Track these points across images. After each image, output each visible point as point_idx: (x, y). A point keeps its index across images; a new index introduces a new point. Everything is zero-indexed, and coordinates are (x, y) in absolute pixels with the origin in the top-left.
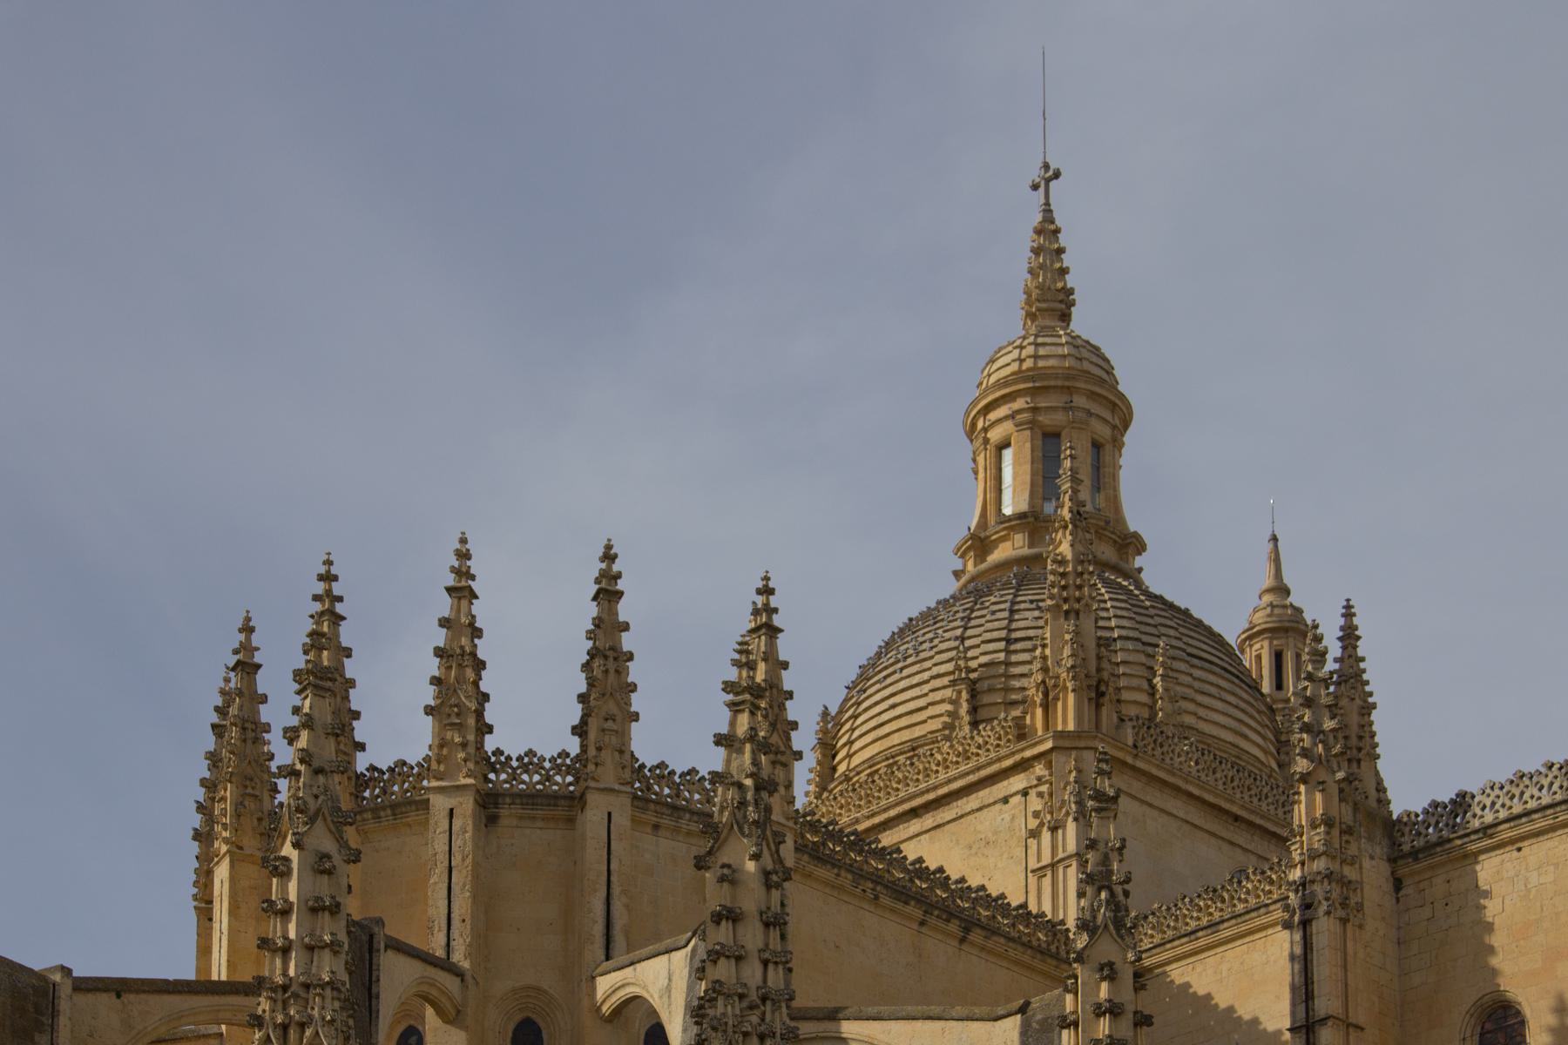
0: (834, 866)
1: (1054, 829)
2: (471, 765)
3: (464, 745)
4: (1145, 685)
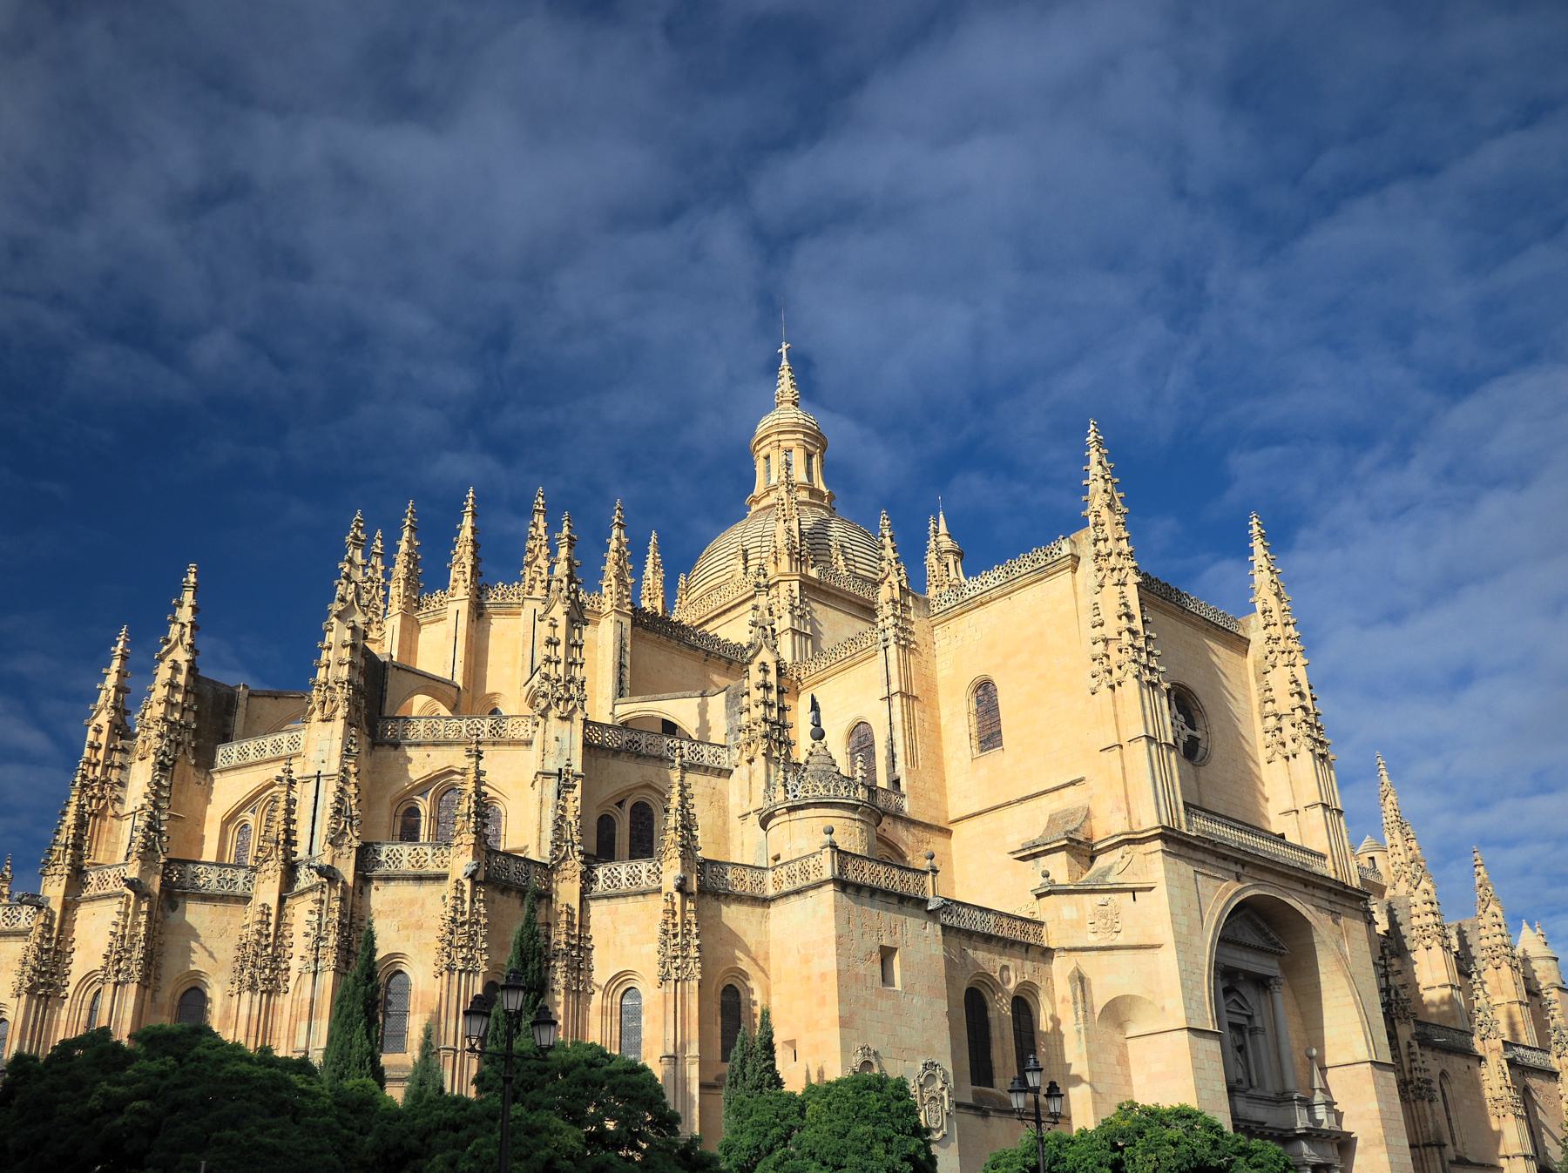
2: (468, 590)
3: (465, 581)
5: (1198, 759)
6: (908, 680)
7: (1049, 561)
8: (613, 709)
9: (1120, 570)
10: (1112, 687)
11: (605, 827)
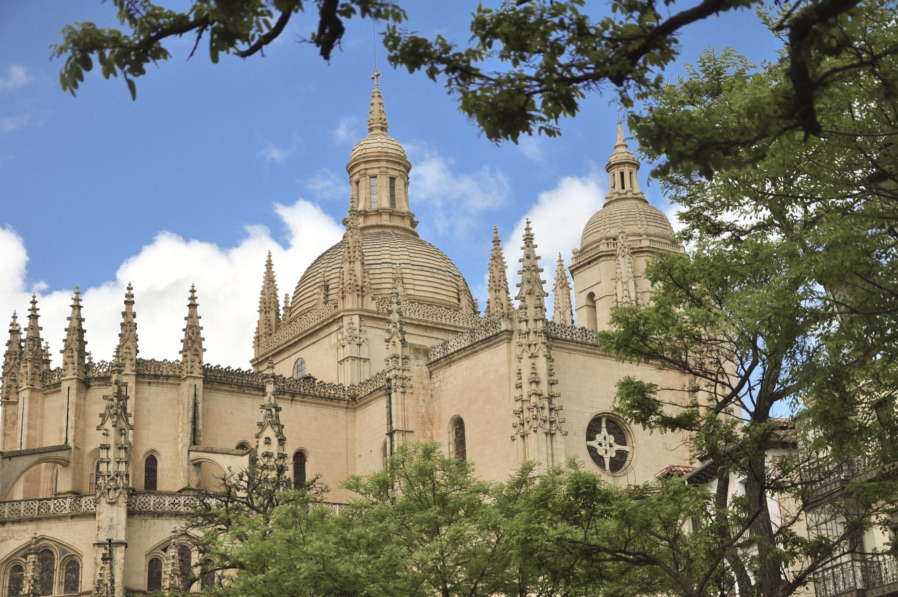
0: (228, 384)
1: (343, 346)
2: (76, 371)
3: (73, 364)
4: (391, 281)
5: (613, 474)
6: (405, 419)
7: (494, 333)
8: (189, 453)
9: (535, 345)
10: (523, 437)
11: (154, 566)
